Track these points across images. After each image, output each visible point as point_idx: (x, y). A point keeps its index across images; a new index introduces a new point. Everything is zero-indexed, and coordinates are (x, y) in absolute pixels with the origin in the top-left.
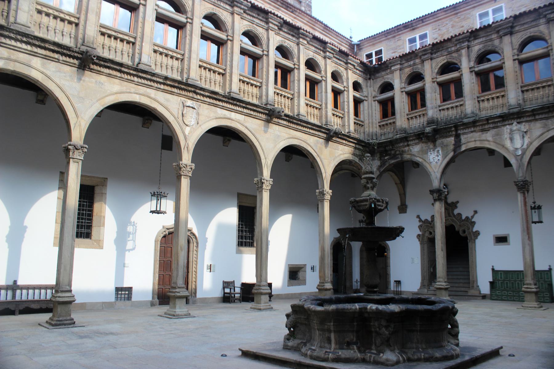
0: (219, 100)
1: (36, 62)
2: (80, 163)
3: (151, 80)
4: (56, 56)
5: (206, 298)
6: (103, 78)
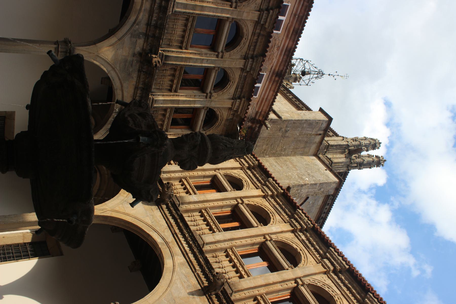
1: (180, 259)
4: (197, 268)
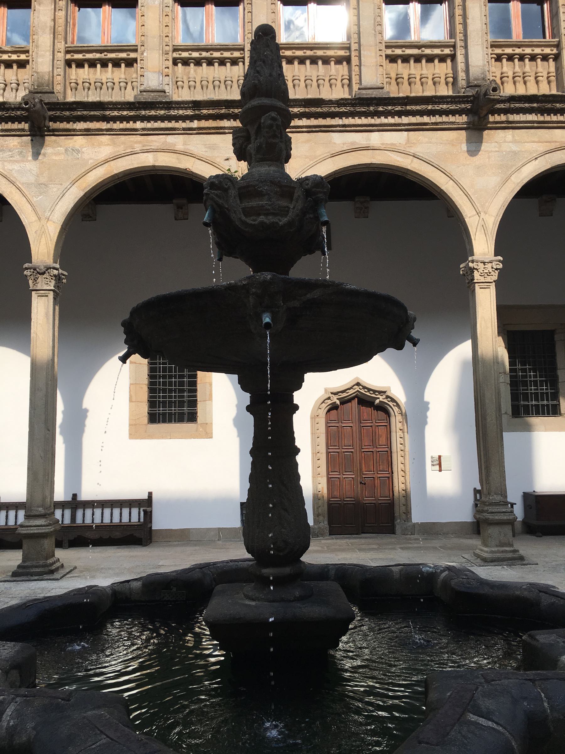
0: (333, 115)
2: (51, 295)
3: (170, 118)
5: (434, 523)
6: (79, 141)
